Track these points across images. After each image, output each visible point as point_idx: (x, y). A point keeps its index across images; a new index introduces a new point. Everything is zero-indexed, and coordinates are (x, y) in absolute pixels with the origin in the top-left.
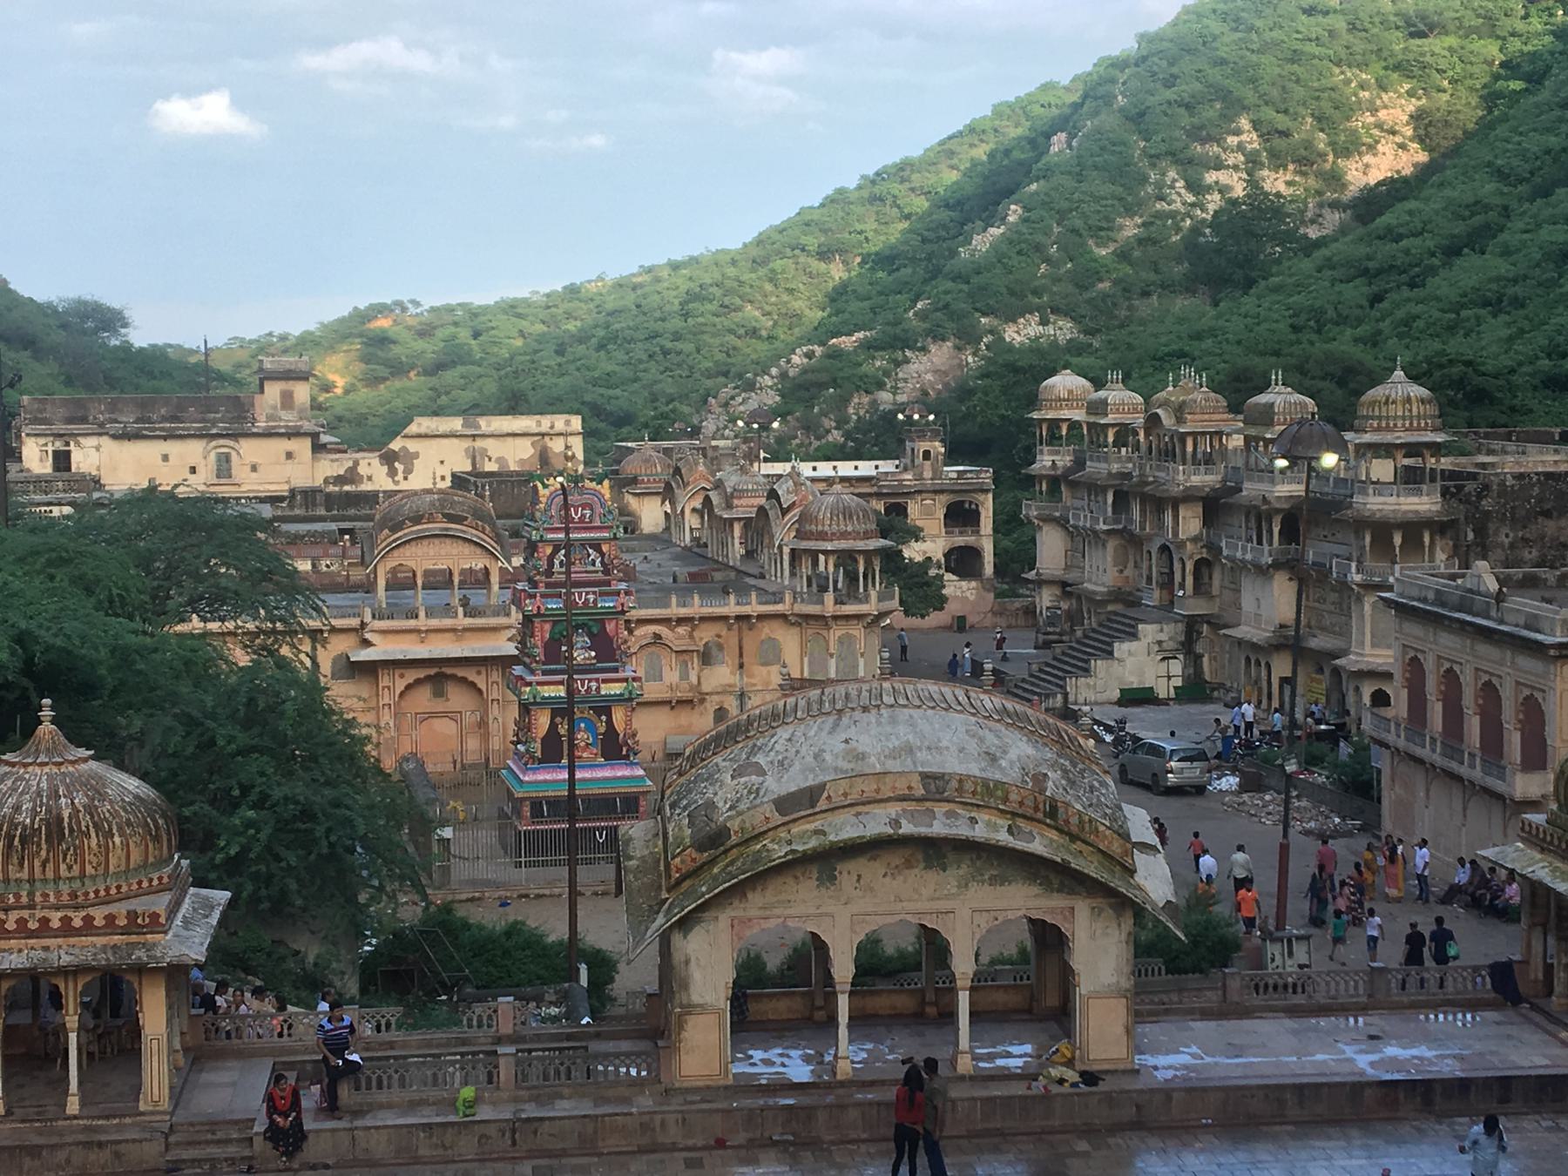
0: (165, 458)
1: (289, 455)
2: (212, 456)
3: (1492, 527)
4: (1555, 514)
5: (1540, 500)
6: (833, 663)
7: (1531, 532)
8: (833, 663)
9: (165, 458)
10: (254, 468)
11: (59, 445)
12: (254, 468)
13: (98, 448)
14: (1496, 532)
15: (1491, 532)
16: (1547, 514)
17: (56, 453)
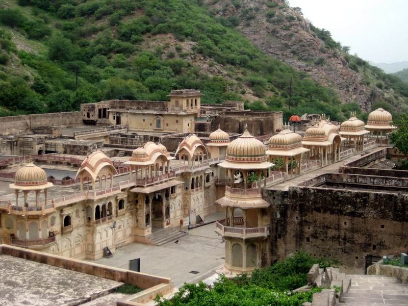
0: (144, 120)
1: (177, 121)
2: (155, 121)
3: (289, 213)
4: (322, 211)
5: (315, 202)
6: (28, 234)
7: (309, 217)
8: (28, 234)
9: (144, 120)
10: (167, 125)
11: (118, 115)
12: (167, 125)
13: (127, 116)
14: (292, 216)
15: (289, 216)
16: (318, 210)
17: (117, 117)
